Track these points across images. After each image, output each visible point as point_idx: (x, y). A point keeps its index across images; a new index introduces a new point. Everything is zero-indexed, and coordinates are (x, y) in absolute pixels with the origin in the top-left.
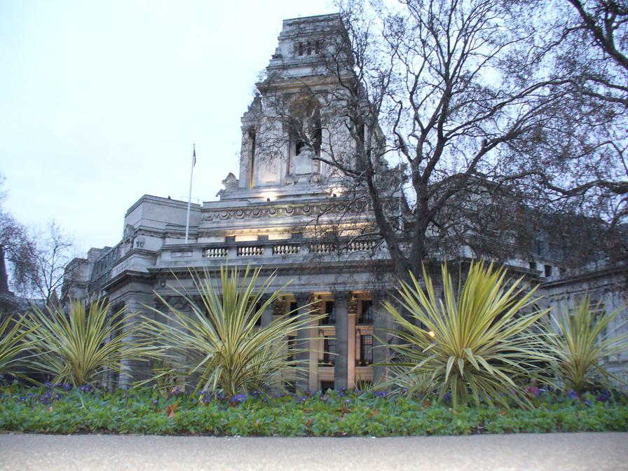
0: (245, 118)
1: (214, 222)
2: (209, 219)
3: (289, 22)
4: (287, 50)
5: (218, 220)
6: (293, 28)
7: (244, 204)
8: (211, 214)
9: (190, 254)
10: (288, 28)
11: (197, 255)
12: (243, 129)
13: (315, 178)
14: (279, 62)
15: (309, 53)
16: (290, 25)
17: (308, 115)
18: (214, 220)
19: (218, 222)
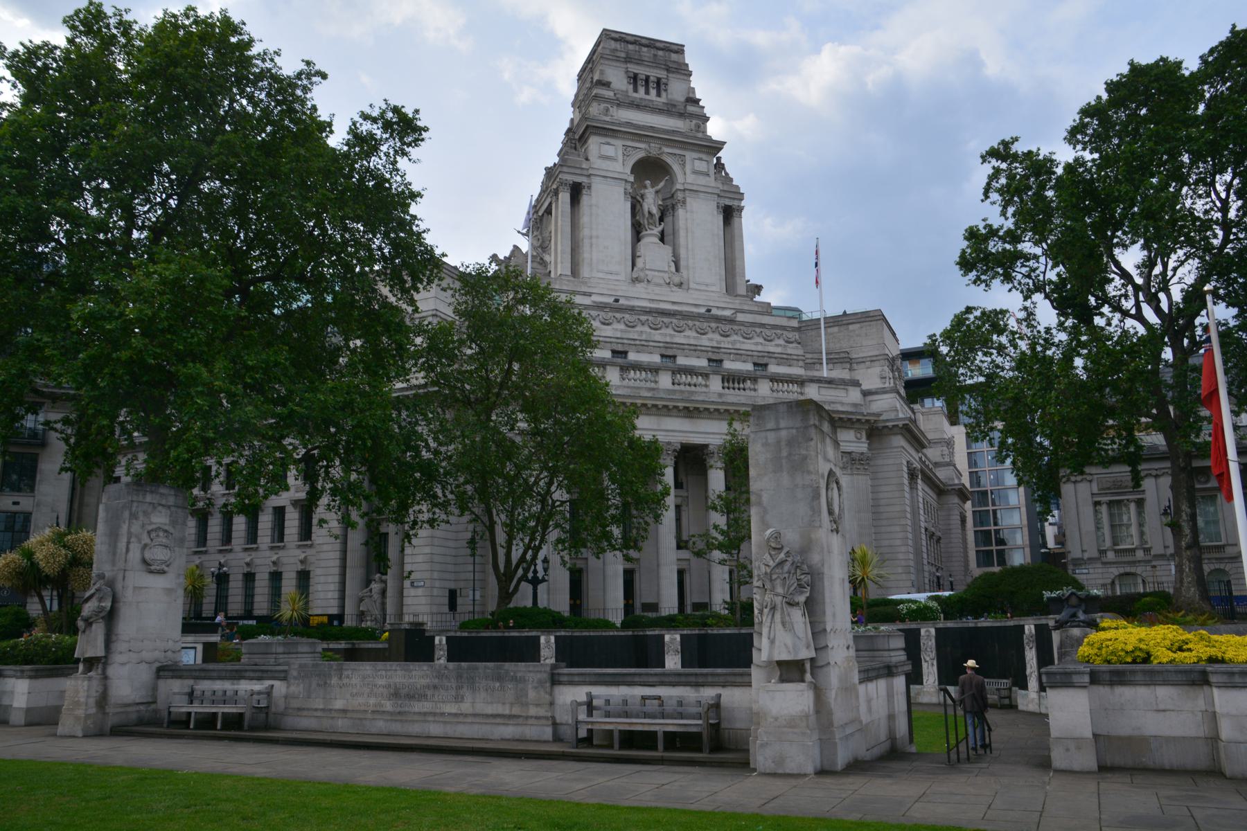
3: (613, 35)
10: (613, 45)
13: (677, 279)
14: (611, 94)
15: (647, 92)
16: (615, 40)
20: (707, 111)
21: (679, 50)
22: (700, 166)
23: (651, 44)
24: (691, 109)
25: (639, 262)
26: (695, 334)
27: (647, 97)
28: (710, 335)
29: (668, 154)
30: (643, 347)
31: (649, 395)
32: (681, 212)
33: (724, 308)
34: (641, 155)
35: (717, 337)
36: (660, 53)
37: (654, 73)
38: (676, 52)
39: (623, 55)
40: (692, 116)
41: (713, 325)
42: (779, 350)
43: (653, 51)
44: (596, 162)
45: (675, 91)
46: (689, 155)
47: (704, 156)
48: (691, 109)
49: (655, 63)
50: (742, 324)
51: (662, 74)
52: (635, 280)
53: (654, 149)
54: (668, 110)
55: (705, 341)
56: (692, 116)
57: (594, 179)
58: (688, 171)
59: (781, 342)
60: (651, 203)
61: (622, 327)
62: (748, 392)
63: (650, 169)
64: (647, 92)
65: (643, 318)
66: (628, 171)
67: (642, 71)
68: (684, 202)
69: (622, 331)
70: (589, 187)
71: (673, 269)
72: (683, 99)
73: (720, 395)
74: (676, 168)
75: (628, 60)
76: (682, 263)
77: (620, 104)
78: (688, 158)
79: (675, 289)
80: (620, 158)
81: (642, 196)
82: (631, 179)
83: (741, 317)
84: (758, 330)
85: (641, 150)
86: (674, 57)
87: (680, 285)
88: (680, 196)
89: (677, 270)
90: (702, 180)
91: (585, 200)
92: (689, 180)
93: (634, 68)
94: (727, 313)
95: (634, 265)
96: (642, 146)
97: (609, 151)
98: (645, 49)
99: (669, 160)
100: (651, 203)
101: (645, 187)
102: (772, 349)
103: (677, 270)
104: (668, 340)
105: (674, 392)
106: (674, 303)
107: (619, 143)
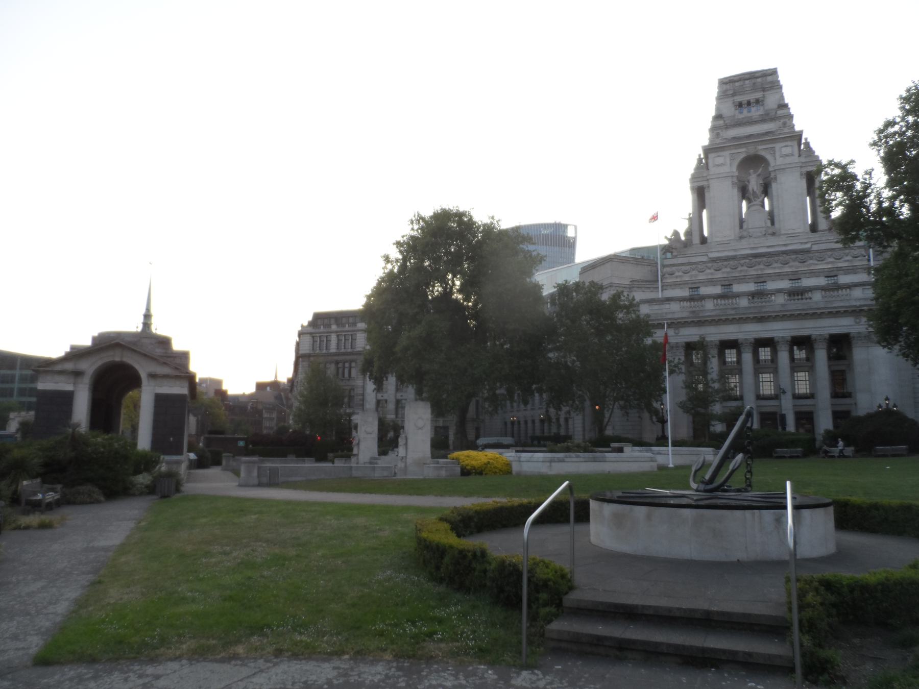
0: (694, 178)
1: (677, 277)
2: (672, 274)
4: (729, 110)
5: (680, 274)
6: (728, 87)
7: (705, 259)
8: (674, 268)
9: (667, 306)
10: (725, 87)
11: (675, 307)
12: (693, 189)
13: (770, 231)
14: (721, 122)
15: (749, 111)
16: (726, 83)
17: (755, 172)
18: (677, 274)
19: (680, 276)
20: (792, 111)
21: (773, 72)
22: (787, 151)
23: (751, 76)
24: (782, 112)
25: (745, 226)
26: (779, 265)
27: (749, 115)
28: (792, 264)
29: (761, 150)
30: (741, 280)
31: (733, 312)
32: (774, 185)
33: (806, 243)
34: (742, 156)
35: (797, 263)
36: (759, 80)
37: (752, 97)
38: (771, 75)
39: (731, 92)
40: (780, 118)
41: (794, 256)
42: (846, 264)
43: (753, 81)
44: (713, 170)
45: (771, 102)
46: (778, 146)
47: (789, 143)
48: (780, 112)
49: (754, 89)
50: (817, 251)
51: (758, 95)
52: (741, 238)
53: (752, 150)
54: (764, 119)
55: (787, 269)
56: (780, 118)
57: (711, 182)
58: (780, 156)
59: (849, 258)
60: (754, 184)
61: (729, 270)
62: (800, 301)
63: (753, 162)
64: (749, 111)
65: (742, 262)
66: (734, 169)
67: (744, 98)
68: (776, 178)
69: (728, 273)
70: (709, 187)
71: (769, 223)
72: (776, 106)
73: (783, 305)
74: (769, 157)
75: (734, 95)
76: (776, 219)
77: (727, 127)
78: (777, 149)
79: (770, 237)
80: (728, 162)
81: (749, 182)
82: (737, 174)
83: (815, 248)
84: (829, 253)
85: (742, 153)
86: (769, 78)
87: (774, 234)
88: (772, 175)
89: (773, 223)
90: (788, 160)
91: (707, 194)
92: (778, 163)
93: (738, 99)
94: (808, 246)
95: (741, 227)
96: (743, 150)
97: (720, 160)
98: (747, 82)
99: (763, 153)
100: (754, 184)
101: (750, 174)
102: (840, 265)
103: (773, 223)
104: (760, 272)
105: (750, 308)
106: (768, 247)
107: (727, 153)
